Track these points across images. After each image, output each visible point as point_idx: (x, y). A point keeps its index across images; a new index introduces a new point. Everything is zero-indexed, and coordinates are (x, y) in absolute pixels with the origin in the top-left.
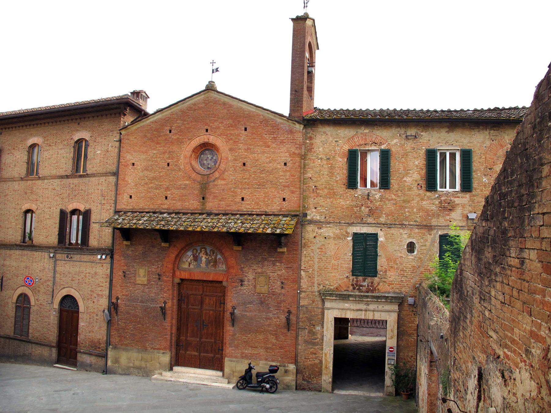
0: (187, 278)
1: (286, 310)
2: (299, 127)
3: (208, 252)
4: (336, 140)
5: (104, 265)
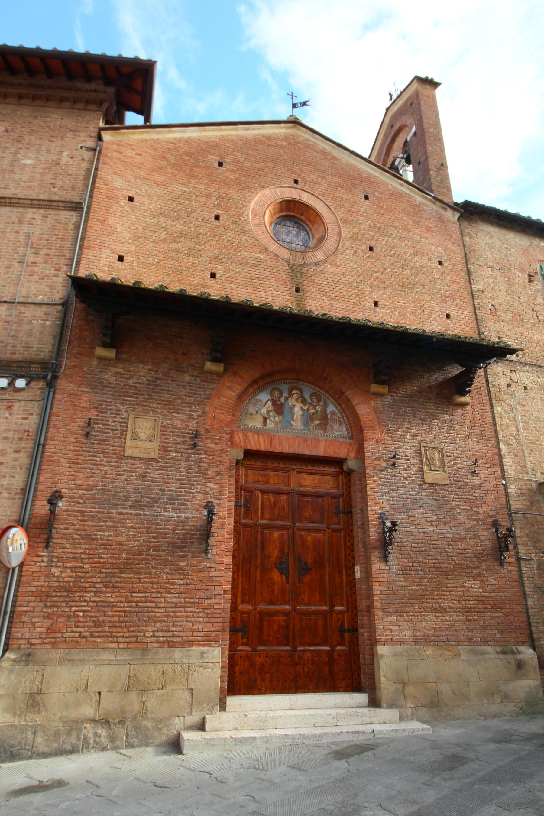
0: (263, 449)
1: (490, 520)
2: (452, 216)
3: (307, 397)
4: (505, 246)
5: (17, 405)
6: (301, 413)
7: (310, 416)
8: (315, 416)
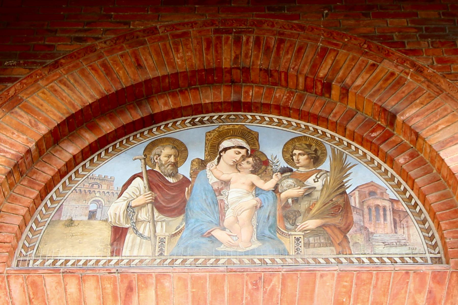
3: (273, 150)
6: (251, 201)
7: (286, 206)
8: (304, 205)
